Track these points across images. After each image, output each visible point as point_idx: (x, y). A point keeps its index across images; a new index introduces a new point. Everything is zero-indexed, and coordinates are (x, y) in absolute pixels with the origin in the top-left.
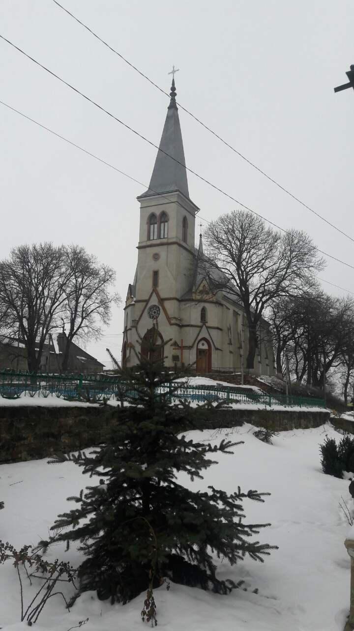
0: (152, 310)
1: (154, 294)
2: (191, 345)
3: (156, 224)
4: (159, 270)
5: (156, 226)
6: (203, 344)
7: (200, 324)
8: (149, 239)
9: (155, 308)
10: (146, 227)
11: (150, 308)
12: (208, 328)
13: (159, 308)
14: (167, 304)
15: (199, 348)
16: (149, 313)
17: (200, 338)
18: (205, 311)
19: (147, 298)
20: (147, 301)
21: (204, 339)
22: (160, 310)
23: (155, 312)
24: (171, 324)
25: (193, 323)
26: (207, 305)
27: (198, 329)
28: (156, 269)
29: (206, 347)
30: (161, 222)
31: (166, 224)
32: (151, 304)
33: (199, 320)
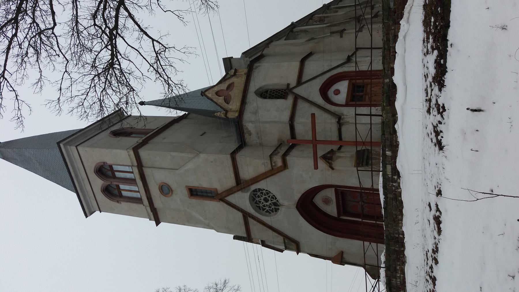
0: (261, 205)
1: (230, 199)
2: (334, 121)
3: (118, 187)
4: (186, 186)
5: (122, 187)
6: (337, 92)
7: (290, 100)
8: (138, 201)
9: (257, 199)
10: (124, 205)
11: (258, 208)
12: (300, 82)
13: (255, 191)
14: (247, 173)
15: (343, 102)
16: (267, 211)
17: (320, 100)
18: (267, 91)
19: (240, 215)
20: (246, 215)
21: (324, 91)
22: (259, 189)
23: (266, 200)
24: (285, 166)
25: (286, 116)
26: (254, 86)
27: (301, 104)
28: (186, 192)
29: (343, 86)
30: (114, 177)
31: (115, 168)
32: (250, 210)
33: (279, 102)
